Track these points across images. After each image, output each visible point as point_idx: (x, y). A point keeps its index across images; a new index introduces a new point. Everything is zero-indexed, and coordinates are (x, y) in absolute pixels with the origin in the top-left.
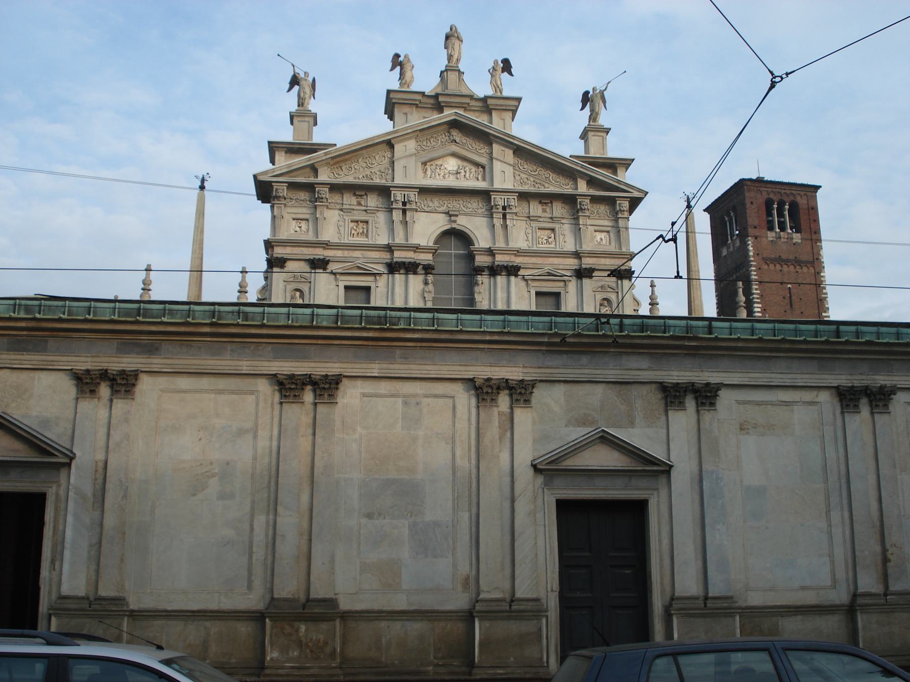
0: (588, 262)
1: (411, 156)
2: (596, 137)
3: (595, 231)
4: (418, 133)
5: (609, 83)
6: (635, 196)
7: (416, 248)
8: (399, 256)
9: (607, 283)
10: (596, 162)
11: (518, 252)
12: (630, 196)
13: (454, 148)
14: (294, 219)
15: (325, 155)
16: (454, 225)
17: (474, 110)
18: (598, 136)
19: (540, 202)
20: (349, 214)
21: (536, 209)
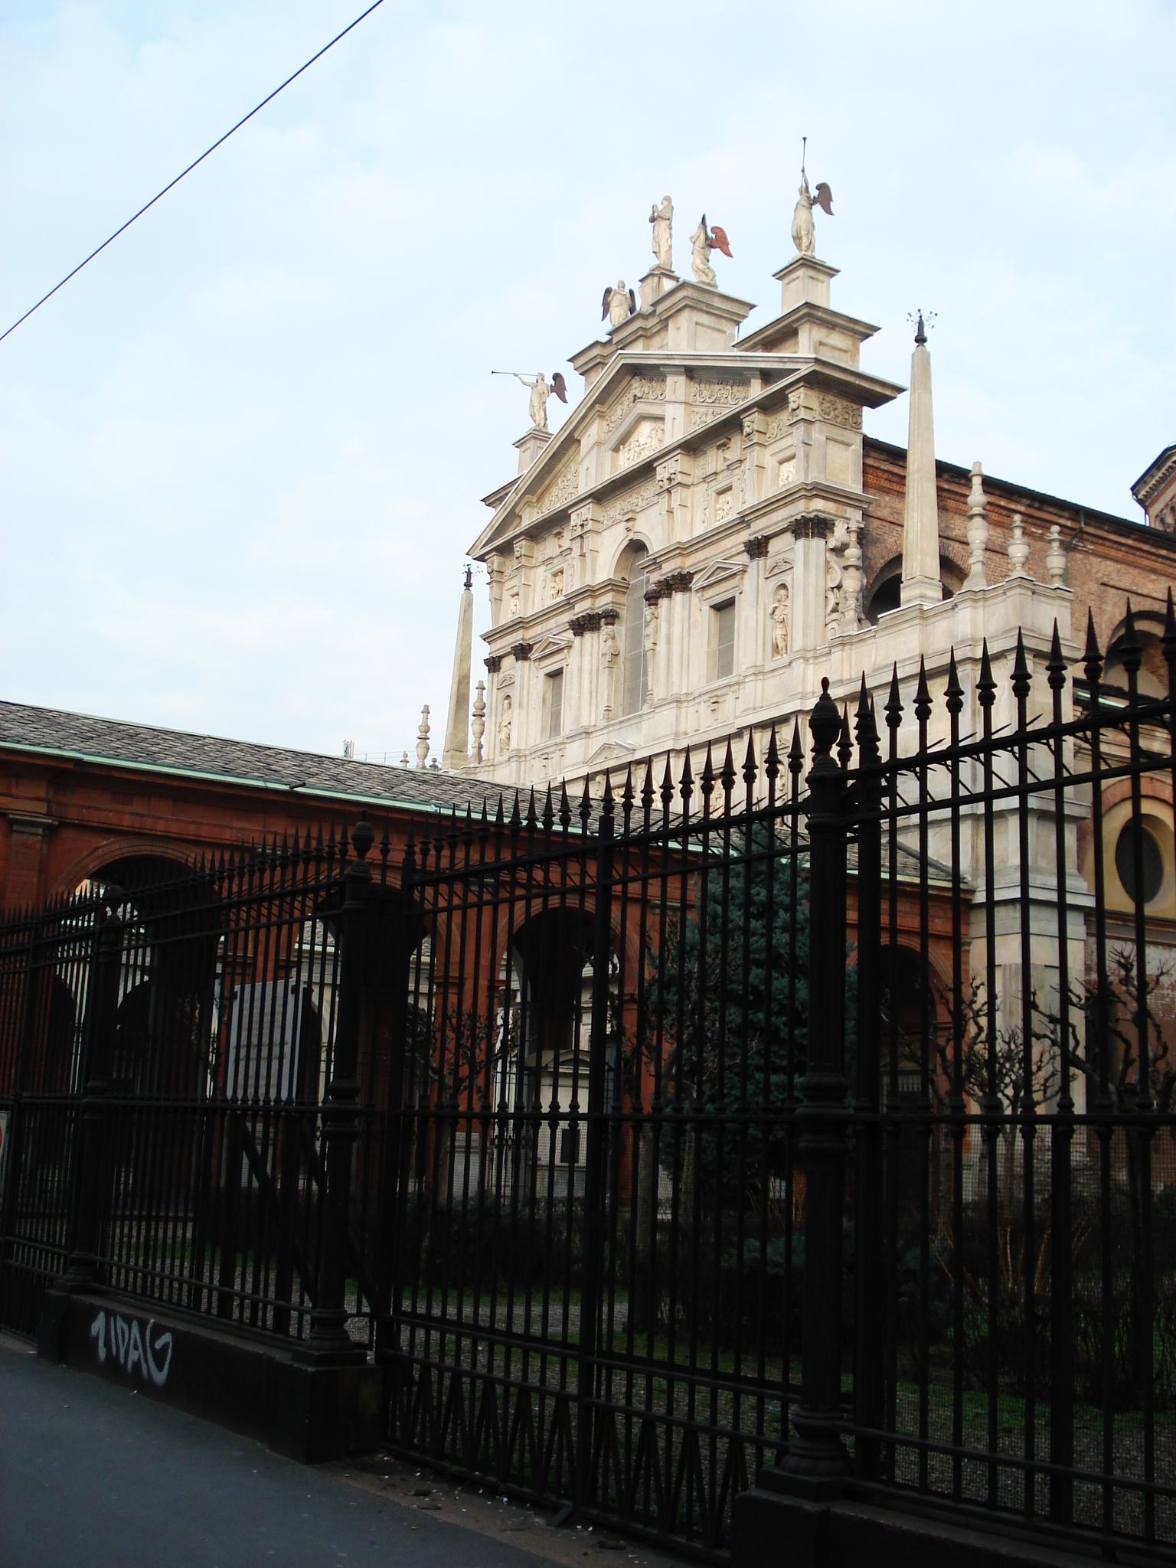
0: (759, 527)
1: (592, 448)
2: (793, 284)
3: (781, 463)
4: (597, 407)
5: (803, 171)
6: (806, 372)
7: (590, 592)
8: (583, 607)
9: (781, 556)
10: (765, 338)
11: (683, 550)
12: (798, 376)
13: (641, 408)
14: (513, 596)
15: (517, 495)
16: (631, 536)
17: (658, 332)
18: (794, 280)
19: (719, 447)
20: (551, 566)
21: (713, 460)
